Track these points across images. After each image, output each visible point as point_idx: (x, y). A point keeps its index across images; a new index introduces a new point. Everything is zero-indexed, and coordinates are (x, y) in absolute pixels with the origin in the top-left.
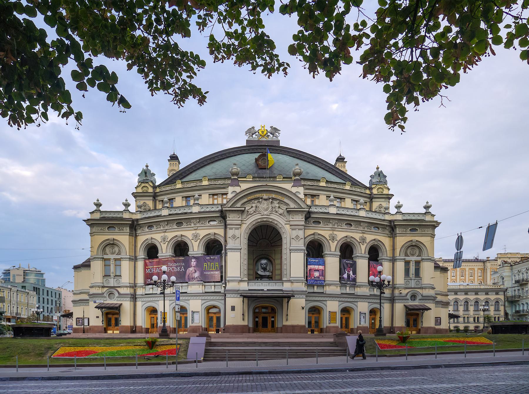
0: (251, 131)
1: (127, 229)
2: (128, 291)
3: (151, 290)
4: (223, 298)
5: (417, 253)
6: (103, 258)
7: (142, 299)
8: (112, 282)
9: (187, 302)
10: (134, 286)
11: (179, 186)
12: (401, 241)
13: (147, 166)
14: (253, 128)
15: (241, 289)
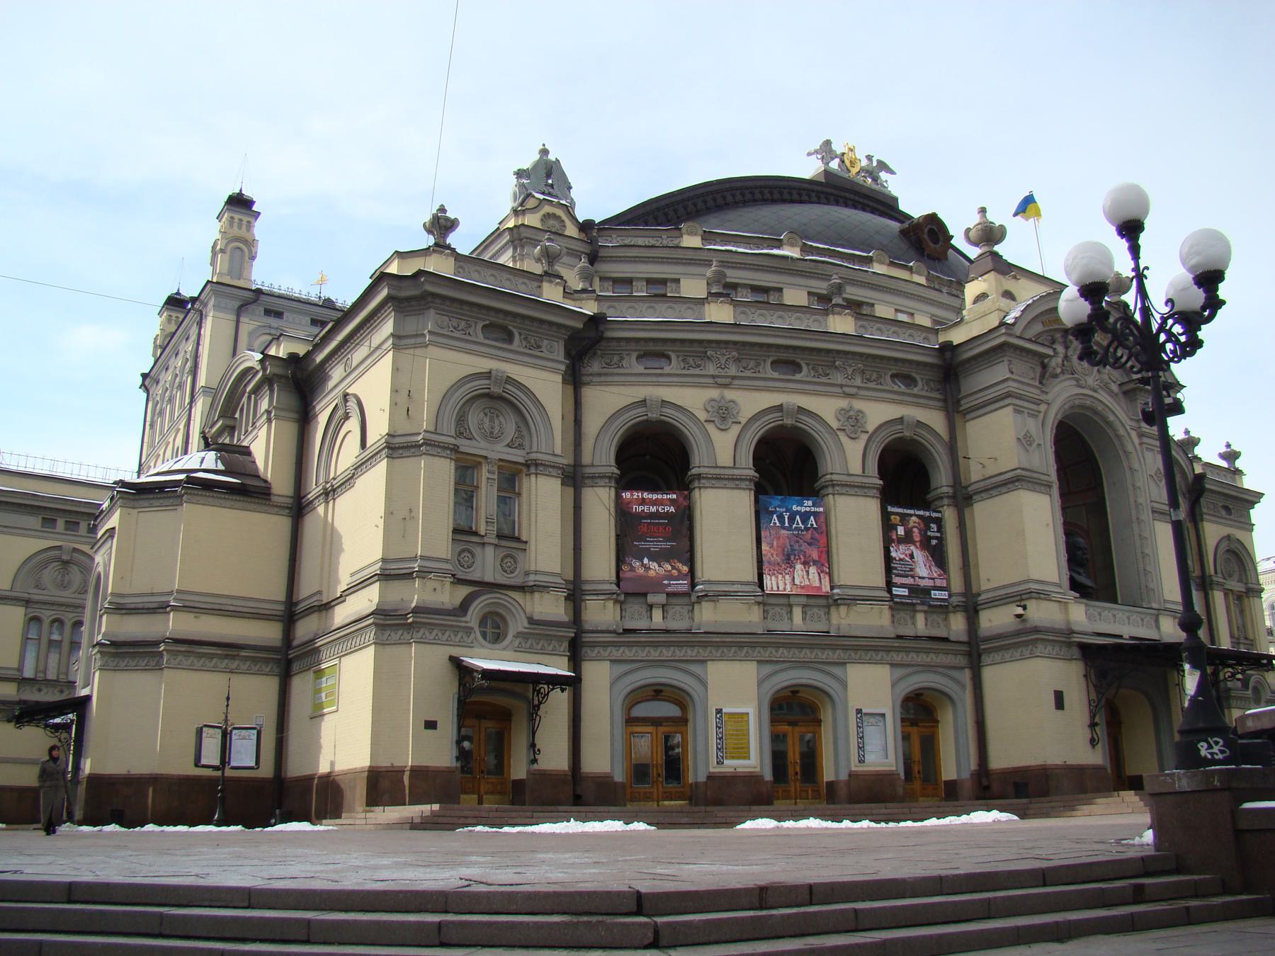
0: (826, 150)
1: (559, 352)
2: (552, 607)
3: (657, 615)
4: (961, 660)
5: (1236, 576)
6: (455, 449)
7: (617, 653)
8: (487, 565)
9: (836, 671)
10: (576, 593)
11: (691, 241)
12: (1213, 532)
13: (544, 152)
14: (828, 143)
15: (1075, 628)
